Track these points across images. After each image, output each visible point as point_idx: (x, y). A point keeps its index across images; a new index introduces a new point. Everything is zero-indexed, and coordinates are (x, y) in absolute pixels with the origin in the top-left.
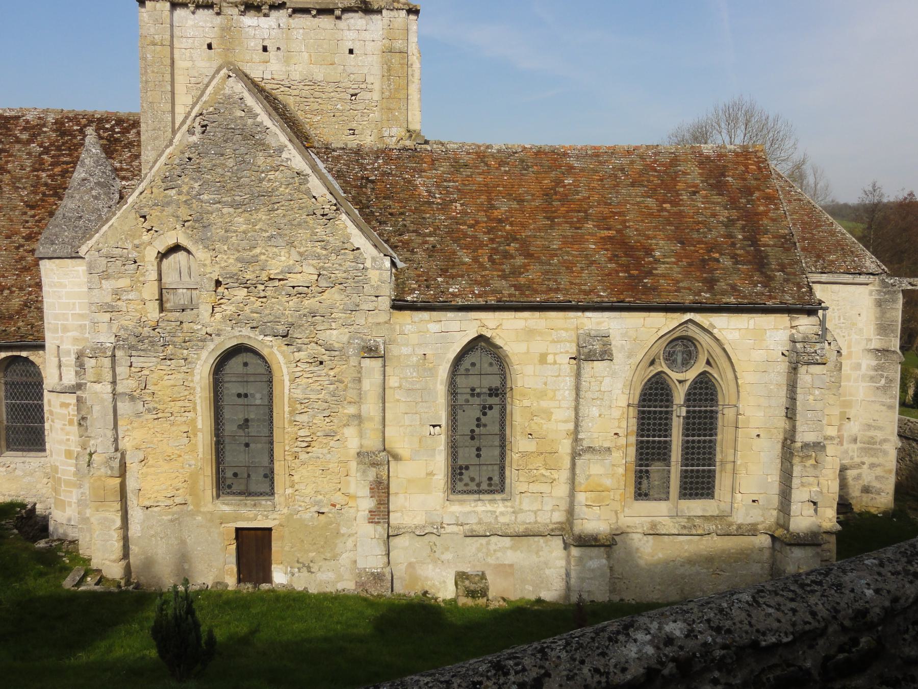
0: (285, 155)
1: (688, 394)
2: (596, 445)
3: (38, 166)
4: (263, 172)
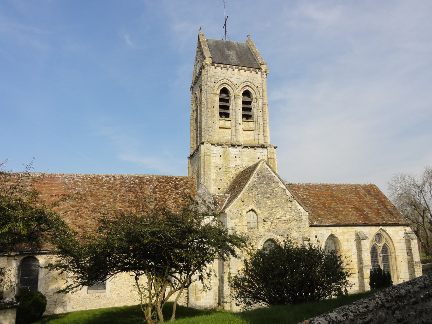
0: (279, 184)
1: (382, 250)
2: (367, 264)
4: (274, 188)
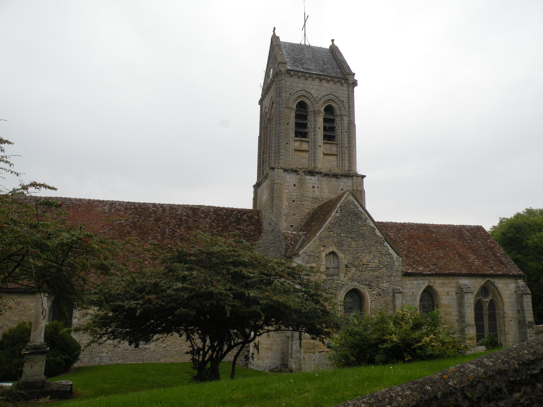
0: (368, 221)
3: (211, 227)
4: (361, 227)
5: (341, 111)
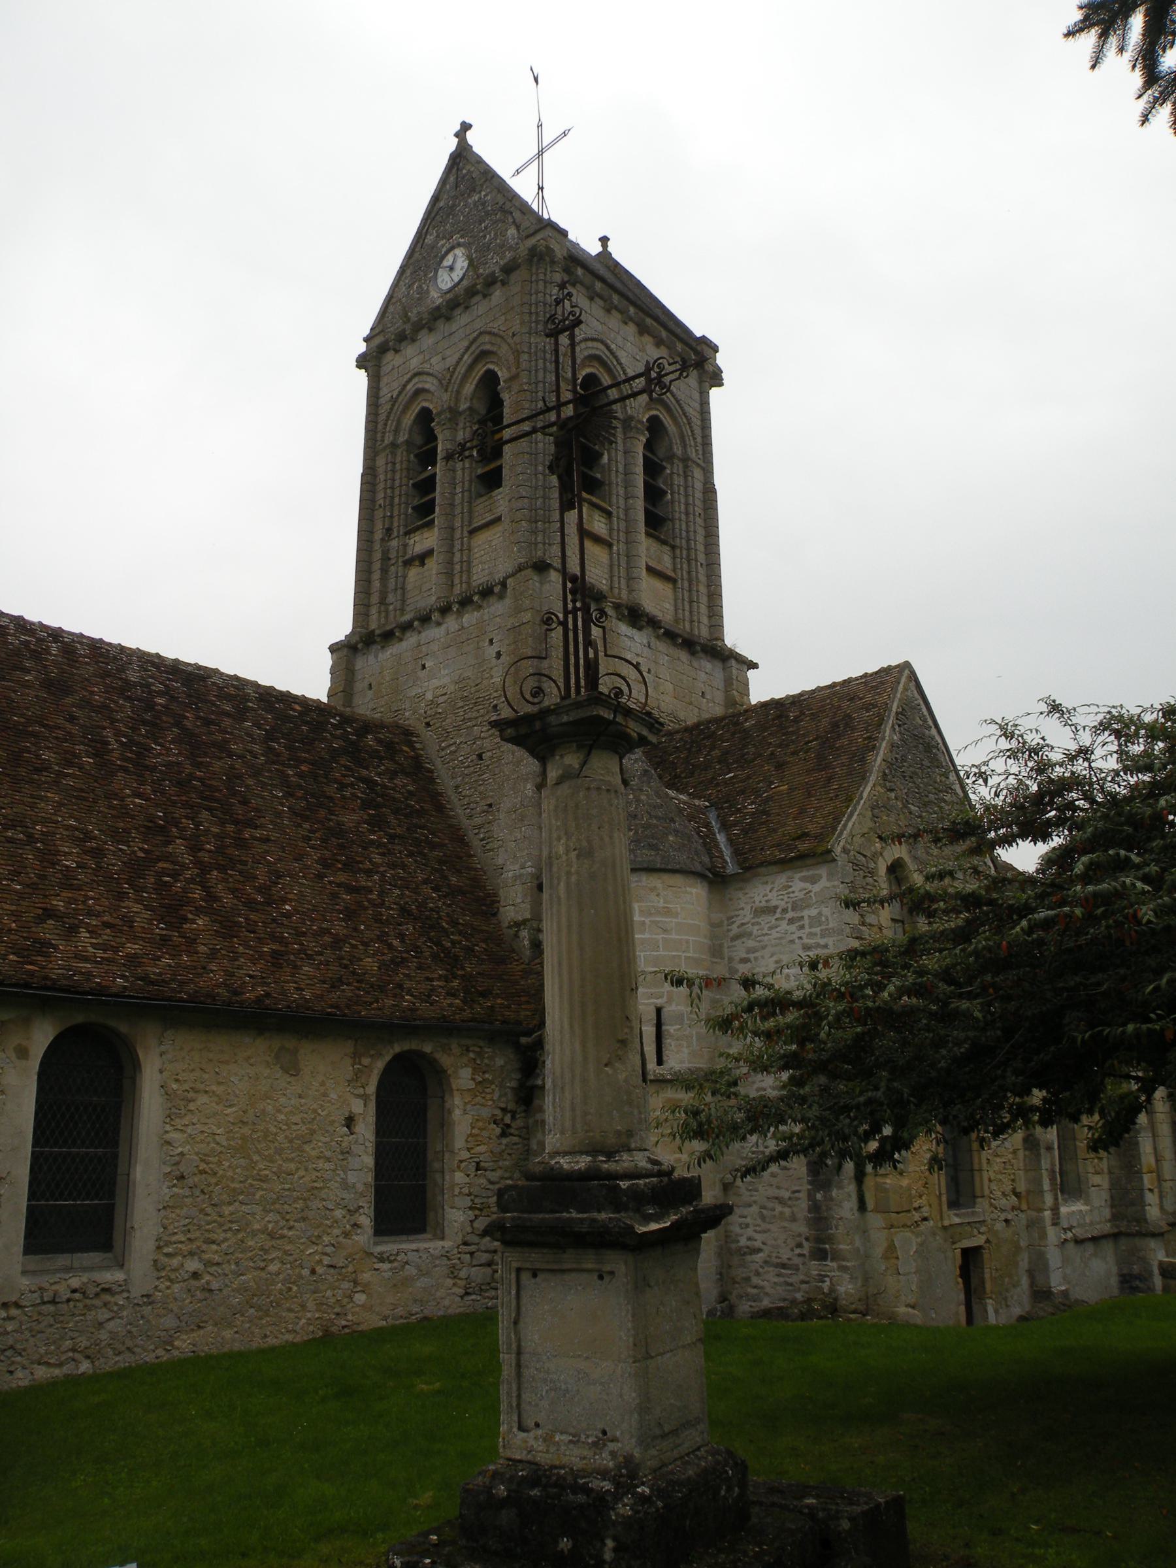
5: (685, 446)
